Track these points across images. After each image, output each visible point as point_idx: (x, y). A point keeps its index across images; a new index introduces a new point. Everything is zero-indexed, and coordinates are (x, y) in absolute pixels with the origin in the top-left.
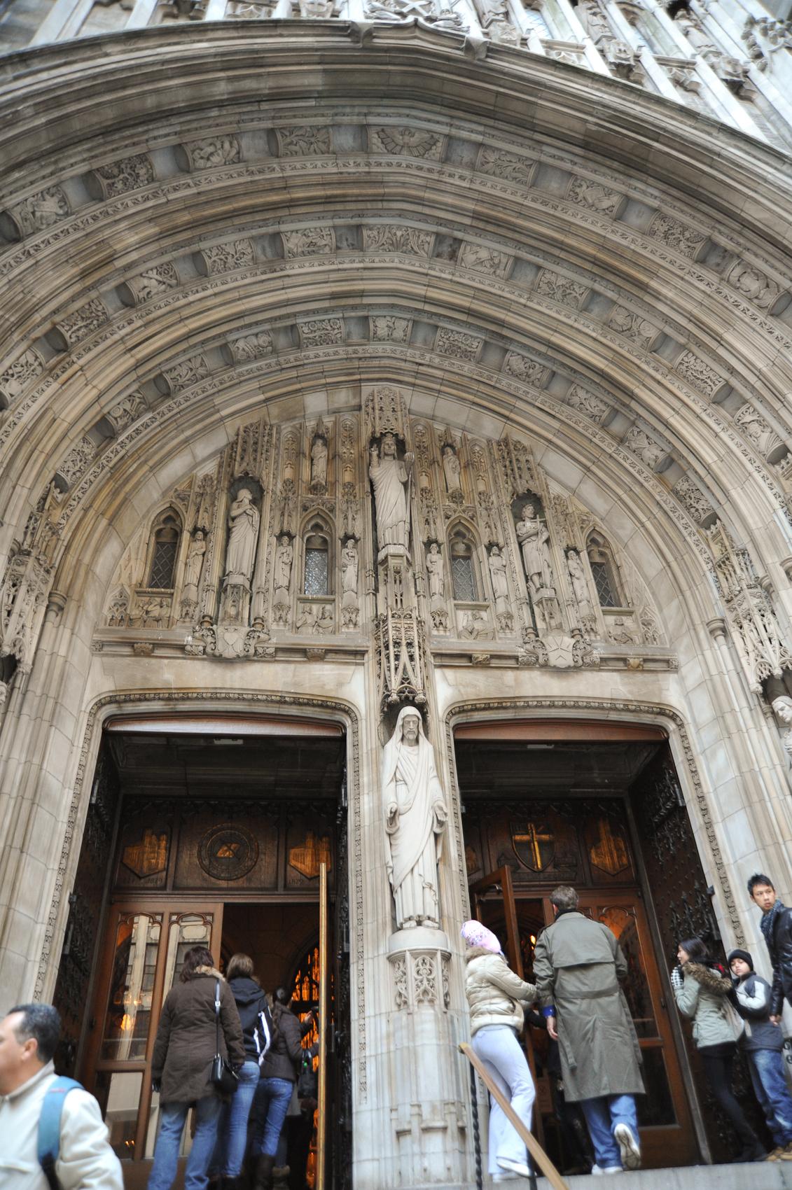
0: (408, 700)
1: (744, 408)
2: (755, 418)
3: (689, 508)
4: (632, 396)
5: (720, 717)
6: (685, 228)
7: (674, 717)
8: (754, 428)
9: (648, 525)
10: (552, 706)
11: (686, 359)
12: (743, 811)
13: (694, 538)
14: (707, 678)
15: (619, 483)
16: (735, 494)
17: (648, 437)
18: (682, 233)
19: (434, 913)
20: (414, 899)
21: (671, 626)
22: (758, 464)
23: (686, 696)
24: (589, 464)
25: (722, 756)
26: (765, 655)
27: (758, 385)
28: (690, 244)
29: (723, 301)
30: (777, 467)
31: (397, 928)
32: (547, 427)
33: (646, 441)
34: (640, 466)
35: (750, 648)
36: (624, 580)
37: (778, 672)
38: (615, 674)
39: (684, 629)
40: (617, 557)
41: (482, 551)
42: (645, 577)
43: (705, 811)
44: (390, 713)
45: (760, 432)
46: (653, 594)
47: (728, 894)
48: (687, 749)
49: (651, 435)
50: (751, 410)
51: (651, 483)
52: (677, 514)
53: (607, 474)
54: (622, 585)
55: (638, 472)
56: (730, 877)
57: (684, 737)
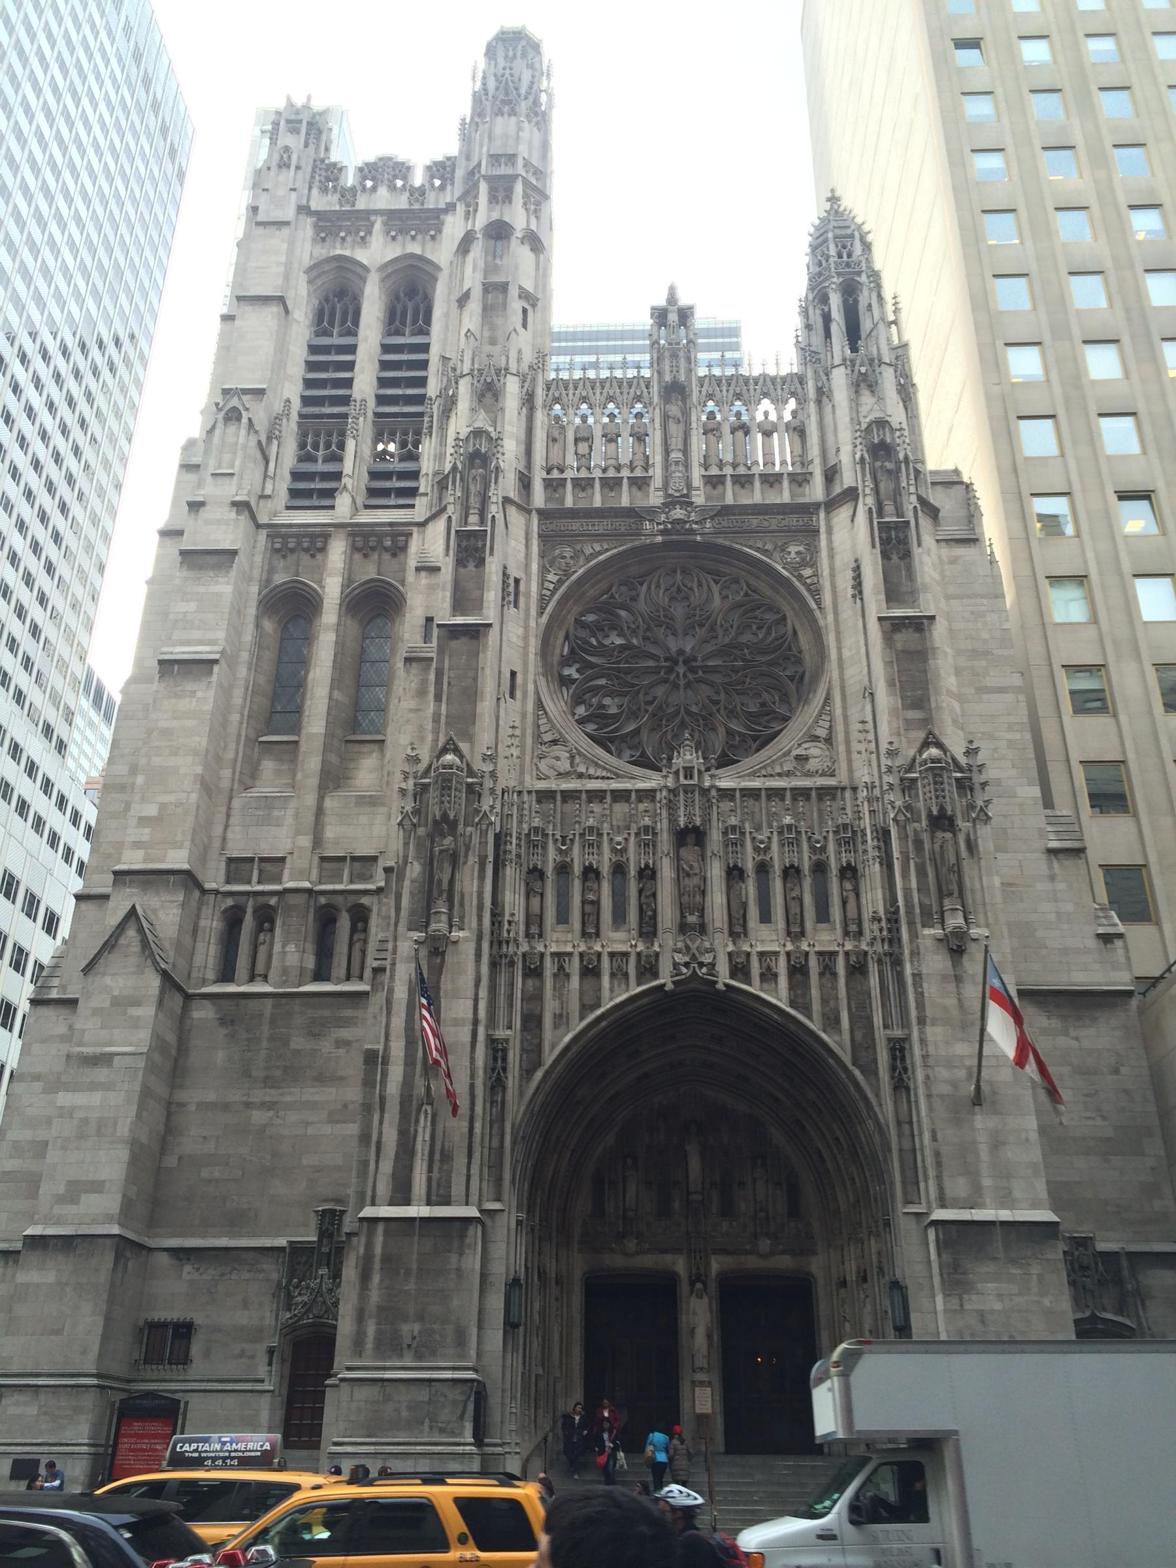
0: (698, 1279)
19: (706, 1366)
20: (701, 1361)
31: (694, 1371)
44: (692, 1284)
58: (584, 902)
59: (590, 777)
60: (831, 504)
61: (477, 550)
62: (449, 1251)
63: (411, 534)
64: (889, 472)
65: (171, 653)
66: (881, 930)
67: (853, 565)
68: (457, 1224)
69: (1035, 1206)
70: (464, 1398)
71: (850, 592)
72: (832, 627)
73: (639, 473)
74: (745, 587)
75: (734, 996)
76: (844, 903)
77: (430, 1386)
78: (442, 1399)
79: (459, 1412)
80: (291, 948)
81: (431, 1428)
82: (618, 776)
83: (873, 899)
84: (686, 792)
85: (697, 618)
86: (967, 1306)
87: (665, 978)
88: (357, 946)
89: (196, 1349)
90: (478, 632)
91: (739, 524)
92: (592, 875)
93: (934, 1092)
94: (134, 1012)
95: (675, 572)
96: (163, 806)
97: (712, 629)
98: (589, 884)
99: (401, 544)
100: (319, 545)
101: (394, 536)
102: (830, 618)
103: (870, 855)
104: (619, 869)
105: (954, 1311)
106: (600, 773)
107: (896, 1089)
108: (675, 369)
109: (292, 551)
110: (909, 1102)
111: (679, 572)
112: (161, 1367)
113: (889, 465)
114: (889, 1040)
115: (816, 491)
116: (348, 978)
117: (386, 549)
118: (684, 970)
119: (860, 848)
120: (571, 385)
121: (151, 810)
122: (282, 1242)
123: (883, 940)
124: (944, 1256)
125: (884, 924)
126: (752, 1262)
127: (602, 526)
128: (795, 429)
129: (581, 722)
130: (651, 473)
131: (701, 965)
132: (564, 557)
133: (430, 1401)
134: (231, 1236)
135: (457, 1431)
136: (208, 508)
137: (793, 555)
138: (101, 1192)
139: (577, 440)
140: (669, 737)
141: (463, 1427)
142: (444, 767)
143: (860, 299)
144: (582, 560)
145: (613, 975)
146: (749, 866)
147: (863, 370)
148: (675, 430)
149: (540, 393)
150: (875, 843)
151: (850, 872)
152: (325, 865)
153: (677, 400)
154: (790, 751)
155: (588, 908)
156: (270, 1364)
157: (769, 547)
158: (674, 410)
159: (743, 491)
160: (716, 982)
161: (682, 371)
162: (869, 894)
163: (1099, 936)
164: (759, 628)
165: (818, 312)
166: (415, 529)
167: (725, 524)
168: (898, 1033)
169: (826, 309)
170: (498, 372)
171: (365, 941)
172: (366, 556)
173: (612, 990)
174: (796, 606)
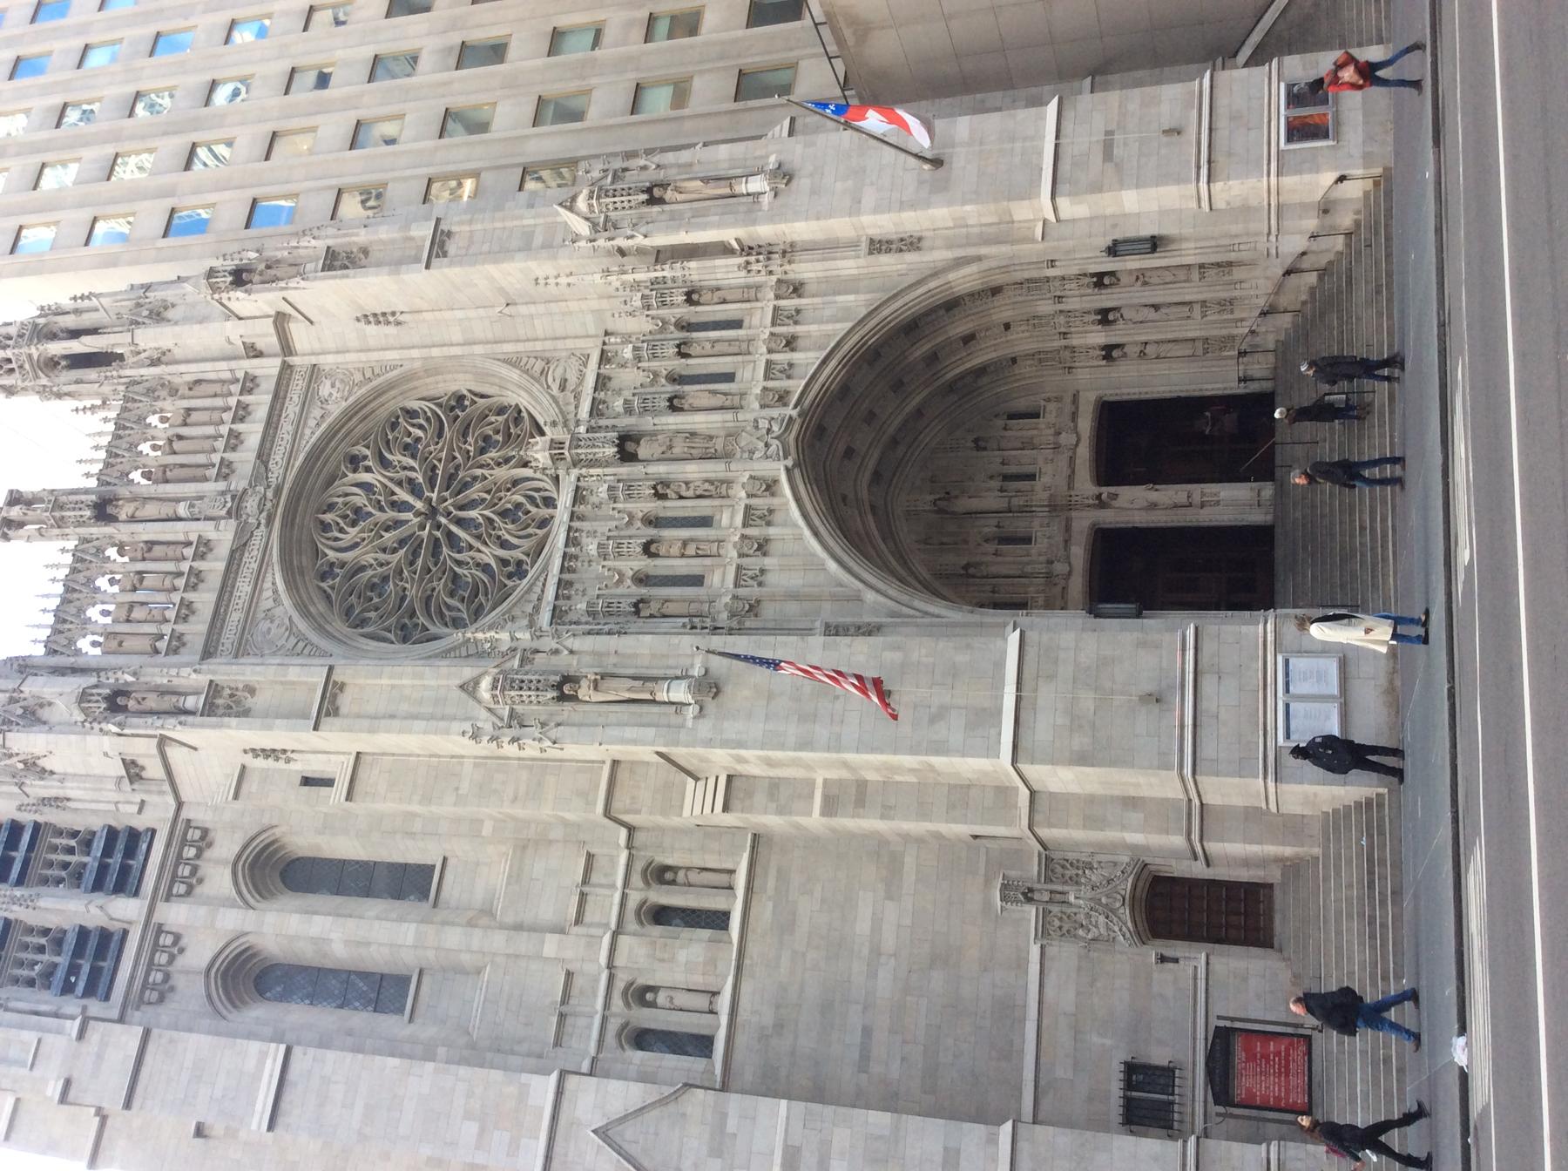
58: (683, 556)
59: (539, 599)
60: (287, 348)
61: (232, 696)
63: (189, 821)
64: (268, 267)
65: (263, 1112)
66: (758, 261)
67: (362, 325)
69: (1043, 118)
71: (391, 330)
72: (425, 352)
73: (189, 552)
74: (359, 447)
75: (807, 402)
76: (724, 302)
80: (682, 956)
82: (545, 569)
83: (726, 271)
84: (578, 447)
85: (381, 498)
87: (777, 469)
88: (694, 877)
89: (1158, 1056)
90: (335, 683)
91: (285, 442)
92: (653, 548)
94: (732, 1125)
95: (322, 522)
96: (468, 1116)
97: (400, 483)
98: (662, 551)
99: (198, 834)
100: (169, 940)
101: (184, 842)
102: (415, 353)
103: (679, 274)
104: (653, 521)
106: (538, 589)
107: (919, 249)
108: (78, 505)
109: (167, 977)
111: (321, 516)
112: (1176, 1108)
113: (262, 267)
114: (870, 253)
115: (268, 368)
116: (731, 888)
117: (198, 856)
118: (773, 448)
119: (670, 284)
120: (59, 626)
121: (472, 1128)
122: (1035, 951)
123: (769, 259)
125: (752, 259)
126: (1084, 452)
127: (244, 587)
128: (190, 389)
129: (477, 613)
130: (193, 537)
131: (769, 431)
132: (269, 629)
134: (1023, 1020)
136: (75, 1075)
137: (332, 391)
138: (958, 1151)
139: (128, 621)
140: (510, 526)
142: (494, 687)
143: (63, 325)
144: (278, 611)
145: (769, 524)
146: (671, 389)
147: (146, 313)
148: (151, 510)
149: (55, 661)
150: (667, 267)
151: (691, 298)
152: (588, 918)
153: (116, 506)
154: (553, 397)
155: (691, 550)
156: (1176, 961)
157: (317, 413)
158: (125, 511)
159: (246, 443)
160: (791, 418)
161: (83, 497)
162: (719, 276)
163: (791, 134)
164: (410, 434)
165: (64, 372)
166: (184, 814)
167: (278, 458)
168: (864, 246)
169: (64, 363)
170: (12, 701)
171: (688, 869)
172: (200, 881)
173: (784, 525)
174: (393, 393)
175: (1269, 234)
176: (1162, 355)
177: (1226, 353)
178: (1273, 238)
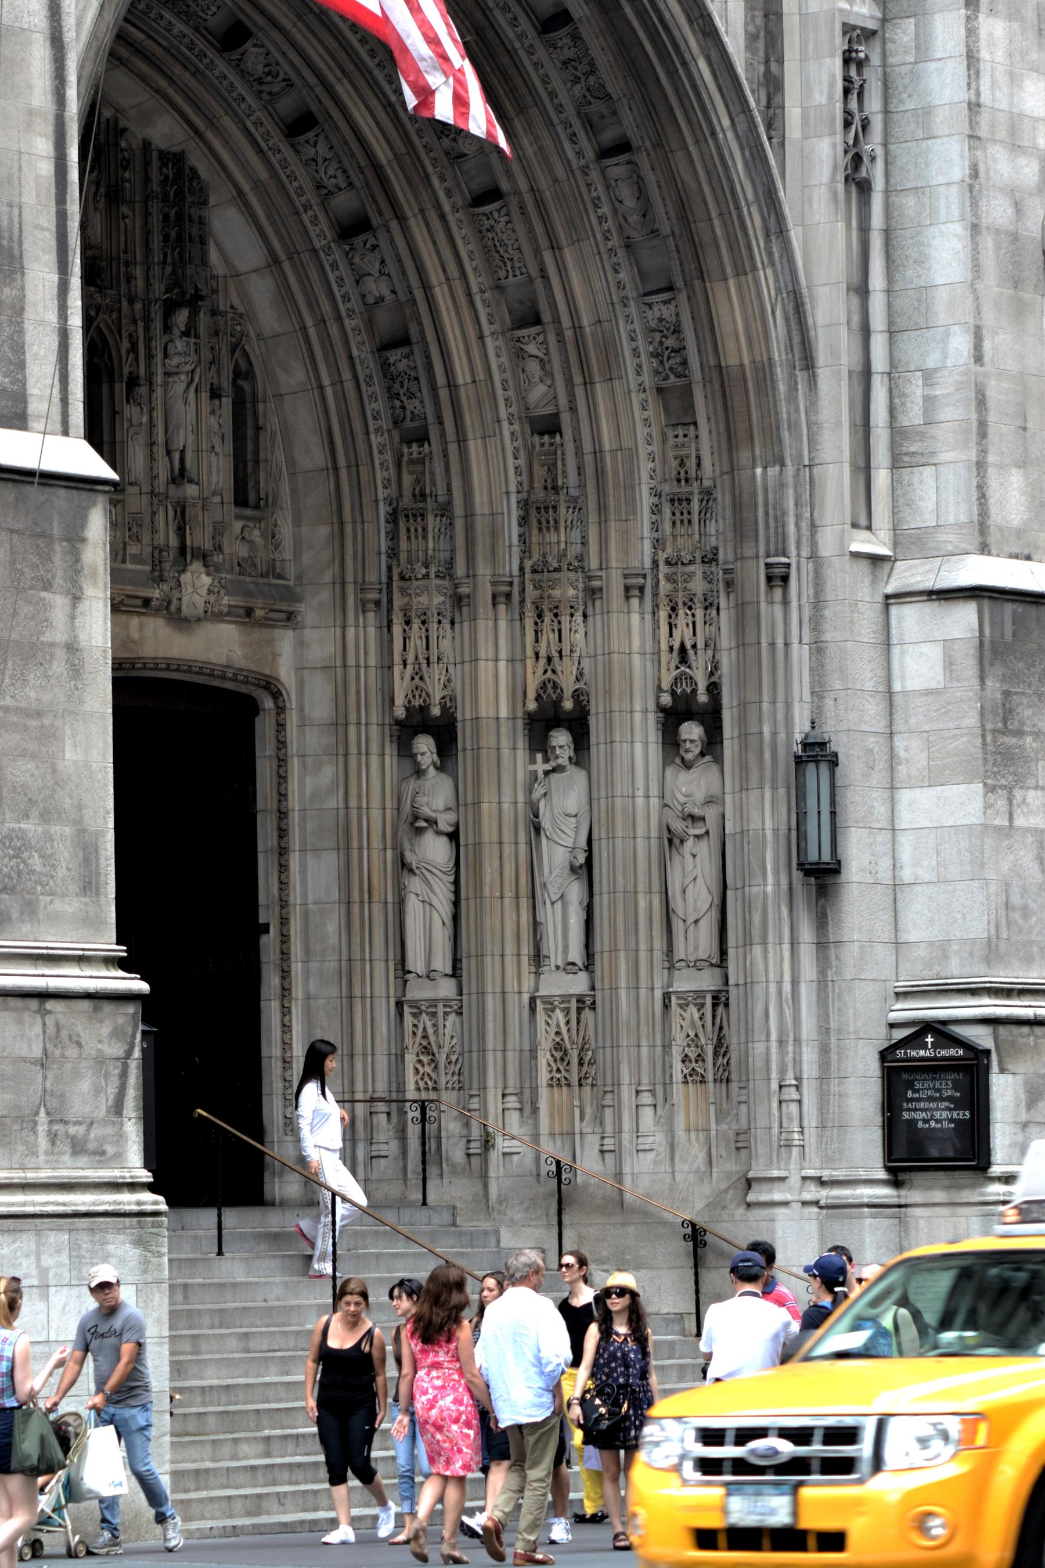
1: (534, 330)
2: (541, 355)
3: (393, 396)
4: (401, 219)
5: (339, 725)
6: (593, 70)
7: (276, 695)
8: (533, 367)
9: (329, 392)
10: (168, 669)
11: (496, 215)
12: (334, 854)
13: (380, 439)
14: (339, 664)
15: (313, 304)
16: (474, 446)
17: (383, 262)
18: (587, 75)
21: (307, 558)
22: (513, 410)
23: (300, 669)
24: (282, 256)
25: (328, 773)
26: (426, 676)
27: (569, 334)
28: (587, 94)
29: (584, 189)
30: (536, 438)
32: (244, 166)
33: (377, 266)
34: (349, 285)
35: (410, 660)
36: (262, 456)
37: (436, 711)
38: (233, 626)
39: (327, 577)
40: (261, 407)
41: (121, 388)
42: (291, 461)
43: (283, 833)
45: (537, 379)
46: (294, 491)
47: (285, 938)
48: (281, 744)
49: (388, 261)
50: (540, 338)
51: (354, 323)
52: (371, 389)
53: (301, 282)
54: (257, 462)
55: (343, 297)
56: (292, 921)
57: (281, 726)
62: (47, 586)
68: (61, 496)
70: (116, 1049)
77: (44, 1013)
78: (72, 1052)
79: (112, 1091)
81: (53, 1137)
86: (1020, 821)
93: (984, 221)
105: (997, 829)
110: (864, 230)
114: (848, 29)
124: (989, 683)
133: (43, 1063)
135: (110, 1150)
141: (120, 1137)
175: (821, 1182)
176: (414, 884)
177: (410, 1059)
178: (812, 1192)
